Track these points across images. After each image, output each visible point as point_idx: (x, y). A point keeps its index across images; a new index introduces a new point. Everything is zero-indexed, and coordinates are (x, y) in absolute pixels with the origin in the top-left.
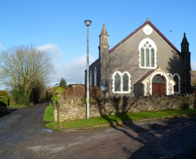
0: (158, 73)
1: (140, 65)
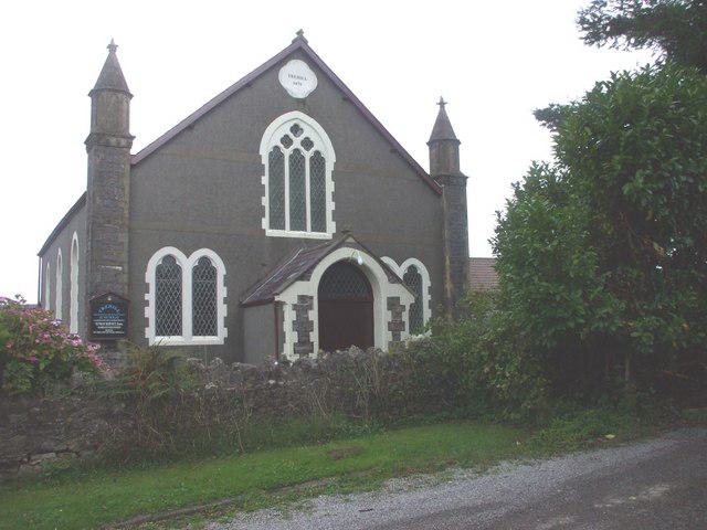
0: (344, 253)
1: (265, 222)
